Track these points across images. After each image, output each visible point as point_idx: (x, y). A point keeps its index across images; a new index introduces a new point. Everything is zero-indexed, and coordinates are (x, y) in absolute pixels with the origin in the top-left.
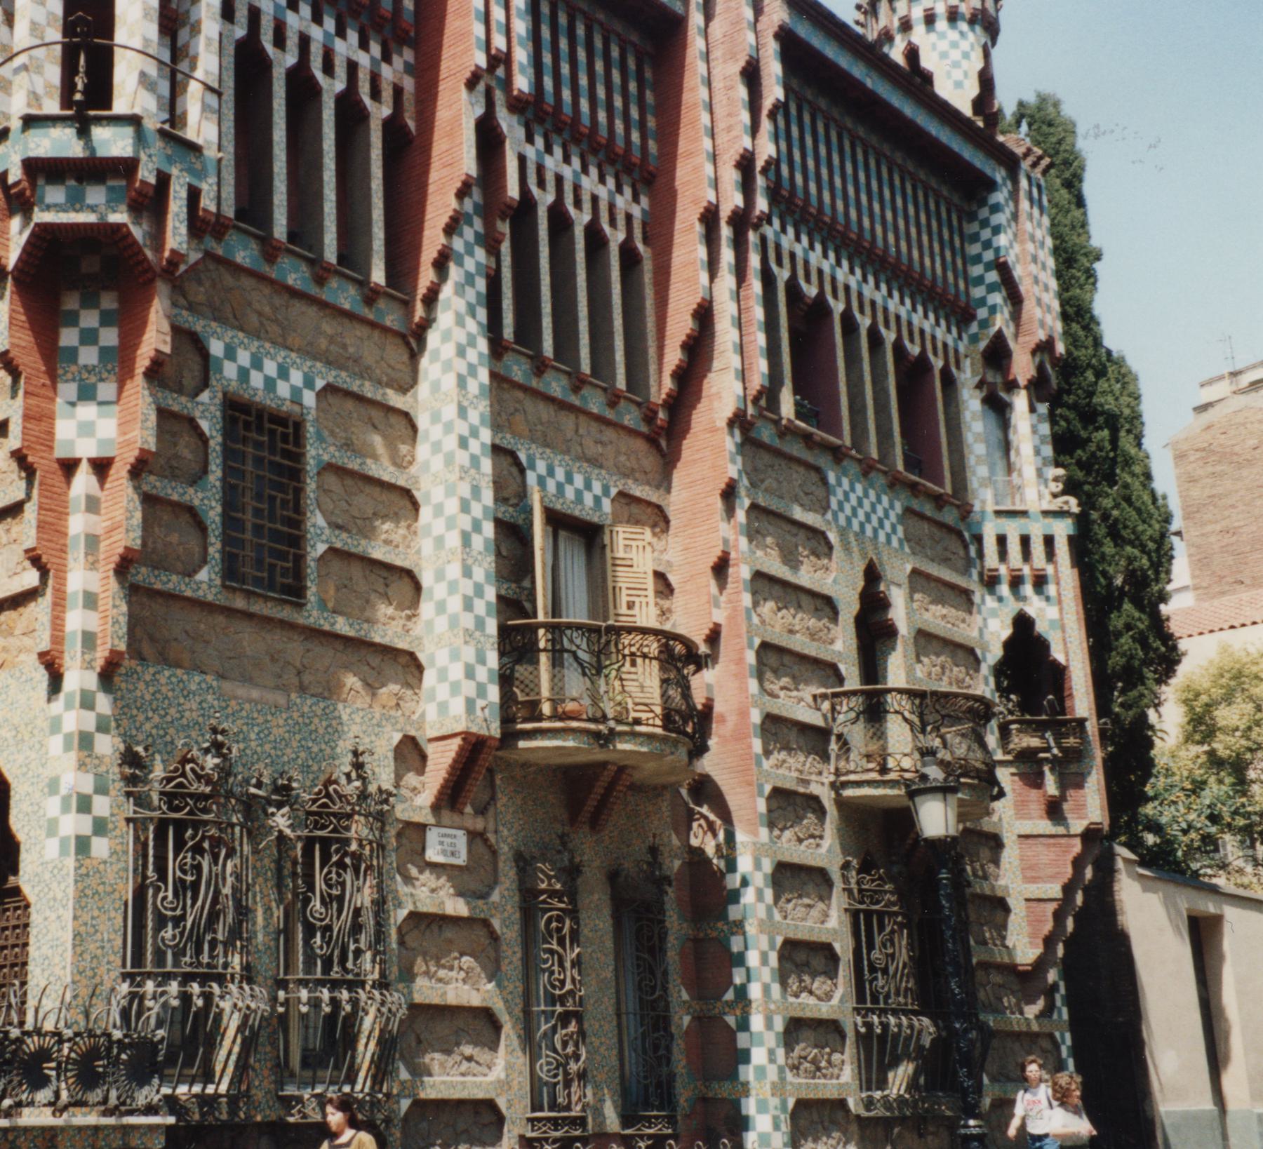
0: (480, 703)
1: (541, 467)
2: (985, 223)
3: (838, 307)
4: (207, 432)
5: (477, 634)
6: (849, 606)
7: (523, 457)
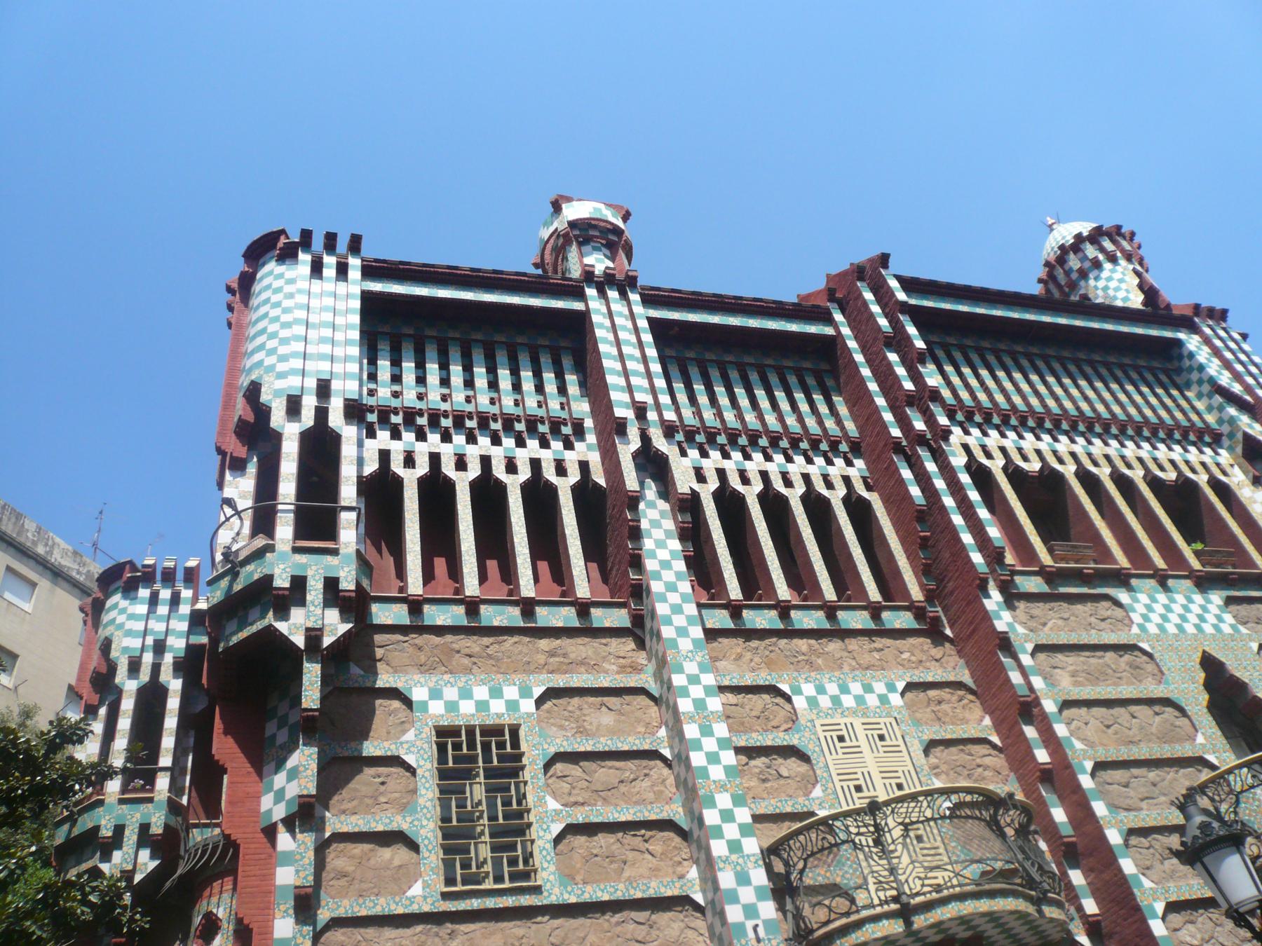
0: (749, 924)
1: (809, 689)
2: (1190, 369)
3: (1069, 470)
4: (414, 765)
5: (734, 857)
6: (1196, 698)
7: (785, 688)
